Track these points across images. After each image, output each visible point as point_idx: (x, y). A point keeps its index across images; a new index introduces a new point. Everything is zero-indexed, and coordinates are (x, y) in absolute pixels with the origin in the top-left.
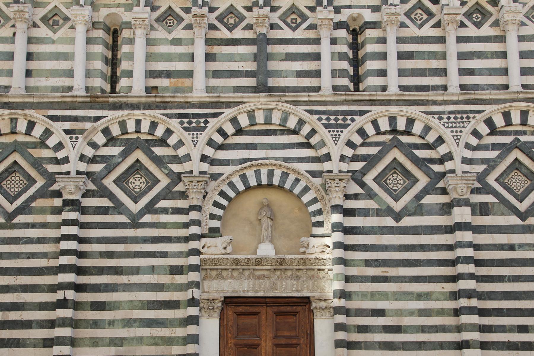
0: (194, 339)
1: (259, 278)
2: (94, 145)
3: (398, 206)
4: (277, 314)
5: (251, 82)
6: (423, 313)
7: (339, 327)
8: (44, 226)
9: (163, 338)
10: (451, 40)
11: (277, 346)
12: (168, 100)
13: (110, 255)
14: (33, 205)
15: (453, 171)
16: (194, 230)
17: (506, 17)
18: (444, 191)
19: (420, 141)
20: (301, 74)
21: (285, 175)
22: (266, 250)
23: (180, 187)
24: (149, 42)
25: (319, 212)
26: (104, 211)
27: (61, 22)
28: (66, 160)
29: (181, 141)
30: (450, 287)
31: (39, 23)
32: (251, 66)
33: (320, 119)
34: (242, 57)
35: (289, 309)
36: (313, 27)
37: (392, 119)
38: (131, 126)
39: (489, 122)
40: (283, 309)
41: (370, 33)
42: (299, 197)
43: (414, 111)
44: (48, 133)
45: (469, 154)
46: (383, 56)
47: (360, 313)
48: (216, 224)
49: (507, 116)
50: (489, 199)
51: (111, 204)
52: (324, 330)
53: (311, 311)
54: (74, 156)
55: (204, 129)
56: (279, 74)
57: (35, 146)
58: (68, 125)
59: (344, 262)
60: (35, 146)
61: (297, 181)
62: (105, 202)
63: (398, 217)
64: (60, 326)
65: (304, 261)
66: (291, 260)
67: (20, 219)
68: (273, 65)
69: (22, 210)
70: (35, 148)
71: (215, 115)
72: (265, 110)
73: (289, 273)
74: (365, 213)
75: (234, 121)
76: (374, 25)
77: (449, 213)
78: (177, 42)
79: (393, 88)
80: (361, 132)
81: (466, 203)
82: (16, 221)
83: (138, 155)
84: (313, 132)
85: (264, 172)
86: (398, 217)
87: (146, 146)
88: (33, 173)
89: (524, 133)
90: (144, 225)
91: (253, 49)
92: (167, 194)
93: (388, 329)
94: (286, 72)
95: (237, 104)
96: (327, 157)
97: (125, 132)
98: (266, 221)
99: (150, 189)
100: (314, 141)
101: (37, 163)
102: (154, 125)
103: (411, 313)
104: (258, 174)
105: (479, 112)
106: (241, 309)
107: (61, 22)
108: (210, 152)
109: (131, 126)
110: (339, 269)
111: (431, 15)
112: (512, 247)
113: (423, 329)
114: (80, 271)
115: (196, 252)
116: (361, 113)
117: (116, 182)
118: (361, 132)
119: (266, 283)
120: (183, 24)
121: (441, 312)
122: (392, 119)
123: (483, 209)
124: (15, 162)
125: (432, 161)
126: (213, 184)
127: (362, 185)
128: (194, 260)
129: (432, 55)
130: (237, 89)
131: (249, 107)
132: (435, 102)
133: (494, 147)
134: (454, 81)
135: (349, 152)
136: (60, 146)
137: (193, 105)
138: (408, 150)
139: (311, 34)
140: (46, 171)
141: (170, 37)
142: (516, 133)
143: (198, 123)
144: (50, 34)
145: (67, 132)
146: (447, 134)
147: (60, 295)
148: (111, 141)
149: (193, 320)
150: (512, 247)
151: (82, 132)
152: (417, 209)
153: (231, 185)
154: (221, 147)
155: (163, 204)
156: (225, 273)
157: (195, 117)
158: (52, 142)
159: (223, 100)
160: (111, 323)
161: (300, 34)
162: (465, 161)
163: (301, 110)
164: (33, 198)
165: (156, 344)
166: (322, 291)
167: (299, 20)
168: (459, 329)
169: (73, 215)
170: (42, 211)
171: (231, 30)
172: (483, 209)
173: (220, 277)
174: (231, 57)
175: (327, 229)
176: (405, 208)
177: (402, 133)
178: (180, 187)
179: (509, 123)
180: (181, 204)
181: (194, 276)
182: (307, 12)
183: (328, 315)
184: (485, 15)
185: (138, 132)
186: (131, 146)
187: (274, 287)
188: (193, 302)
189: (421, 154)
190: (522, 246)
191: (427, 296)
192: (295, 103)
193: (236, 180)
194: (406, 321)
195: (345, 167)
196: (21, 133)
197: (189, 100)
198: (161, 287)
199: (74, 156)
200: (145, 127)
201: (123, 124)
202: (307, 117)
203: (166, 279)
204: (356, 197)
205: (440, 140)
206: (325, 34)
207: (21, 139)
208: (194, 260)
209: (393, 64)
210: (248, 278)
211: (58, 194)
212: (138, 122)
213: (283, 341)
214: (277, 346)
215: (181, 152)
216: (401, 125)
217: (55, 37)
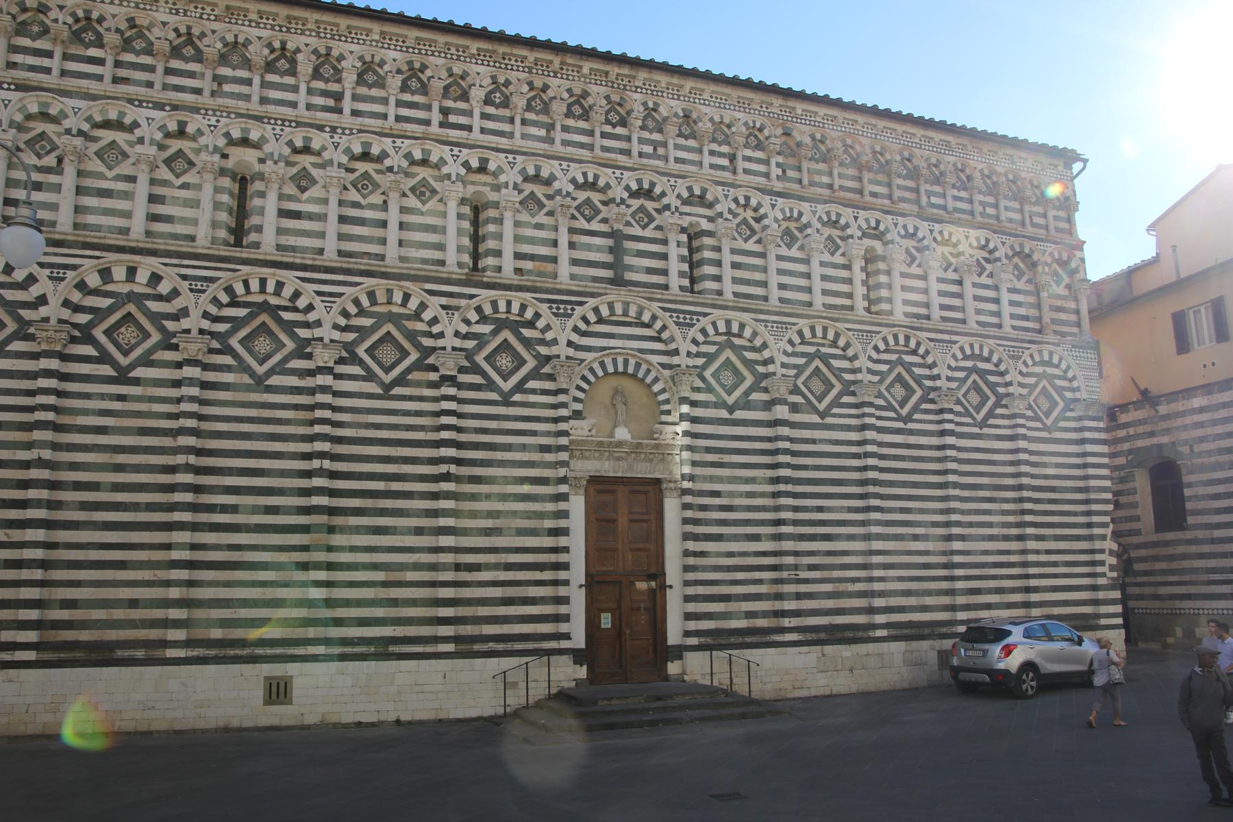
0: (564, 514)
1: (618, 459)
2: (467, 322)
3: (730, 400)
4: (632, 492)
5: (608, 274)
6: (750, 495)
7: (686, 506)
8: (421, 399)
9: (535, 512)
10: (772, 257)
11: (631, 521)
12: (539, 284)
14: (409, 377)
15: (774, 374)
16: (564, 412)
17: (813, 245)
18: (766, 390)
19: (748, 344)
20: (650, 271)
21: (638, 365)
22: (622, 434)
23: (547, 370)
24: (517, 224)
25: (667, 401)
26: (478, 387)
27: (428, 194)
28: (441, 335)
29: (548, 325)
30: (770, 473)
31: (408, 193)
32: (607, 258)
33: (671, 317)
34: (599, 249)
35: (641, 488)
36: (659, 228)
37: (728, 323)
38: (502, 307)
39: (800, 333)
40: (636, 488)
41: (707, 241)
42: (649, 386)
43: (746, 317)
44: (423, 306)
45: (786, 360)
46: (718, 263)
47: (702, 493)
48: (578, 407)
49: (813, 329)
50: (798, 399)
51: (484, 382)
52: (672, 508)
53: (661, 490)
54: (449, 332)
55: (570, 316)
56: (631, 268)
57: (409, 317)
58: (444, 301)
59: (690, 448)
60: (409, 317)
61: (649, 371)
62: (478, 379)
63: (731, 410)
64: (444, 499)
65: (657, 446)
66: (647, 445)
67: (397, 391)
68: (628, 260)
69: (400, 381)
70: (409, 320)
71: (581, 304)
72: (623, 302)
73: (643, 456)
74: (705, 405)
75: (596, 310)
76: (710, 234)
77: (770, 410)
78: (539, 226)
79: (728, 295)
80: (703, 331)
81: (784, 402)
82: (393, 392)
83: (506, 334)
84: (664, 327)
85: (620, 360)
86: (731, 410)
87: (515, 327)
88: (406, 345)
89: (823, 345)
90: (515, 404)
91: (610, 242)
92: (535, 374)
93: (723, 508)
94: (638, 267)
95: (600, 295)
96: (676, 352)
97: (496, 310)
98: (621, 408)
99: (517, 369)
100: (665, 335)
101: (412, 336)
102: (523, 307)
103: (741, 495)
104: (615, 361)
105: (795, 324)
106: (601, 487)
107: (428, 194)
108: (575, 338)
109: (502, 307)
110: (686, 455)
111: (753, 232)
112: (814, 441)
113: (749, 509)
114: (459, 445)
115: (565, 433)
116: (705, 315)
117: (487, 359)
118: (703, 331)
119: (623, 464)
120: (545, 210)
121: (763, 495)
122: (728, 323)
124: (388, 333)
125: (757, 362)
126: (577, 369)
127: (703, 379)
128: (563, 441)
129: (754, 268)
130: (595, 279)
131: (610, 298)
132: (762, 312)
133: (803, 355)
134: (775, 294)
135: (694, 349)
136: (435, 321)
137: (560, 292)
138: (737, 350)
139: (658, 235)
140: (421, 344)
141: (534, 221)
142: (818, 345)
143: (565, 309)
144: (419, 205)
145: (444, 307)
146: (771, 341)
147: (443, 468)
148: (483, 319)
149: (563, 497)
150: (814, 441)
151: (457, 308)
152: (748, 406)
153: (592, 370)
155: (532, 384)
156: (587, 454)
157: (563, 302)
158: (427, 316)
159: (588, 290)
160: (488, 497)
161: (648, 233)
162: (783, 365)
163: (656, 305)
164: (409, 370)
165: (529, 518)
166: (671, 473)
167: (646, 220)
168: (777, 509)
169: (452, 391)
170: (418, 384)
171: (589, 221)
172: (795, 408)
173: (583, 457)
174: (588, 248)
175: (674, 417)
176: (736, 402)
177: (735, 335)
178: (547, 370)
179: (814, 336)
180: (548, 385)
181: (564, 456)
182: (654, 214)
183: (675, 494)
184: (793, 239)
185: (508, 312)
186: (501, 325)
187: (630, 468)
188: (563, 480)
189: (750, 355)
190: (822, 441)
191: (752, 480)
193: (596, 366)
194: (737, 502)
195: (691, 362)
196: (396, 304)
197: (558, 286)
199: (449, 332)
200: (515, 308)
201: (494, 304)
202: (660, 313)
203: (536, 457)
204: (698, 390)
205: (765, 346)
206: (673, 237)
207: (395, 309)
208: (563, 441)
209: (728, 273)
210: (608, 459)
211: (434, 369)
212: (509, 303)
213: (636, 517)
214: (631, 521)
215: (549, 336)
216: (735, 329)
217: (424, 209)
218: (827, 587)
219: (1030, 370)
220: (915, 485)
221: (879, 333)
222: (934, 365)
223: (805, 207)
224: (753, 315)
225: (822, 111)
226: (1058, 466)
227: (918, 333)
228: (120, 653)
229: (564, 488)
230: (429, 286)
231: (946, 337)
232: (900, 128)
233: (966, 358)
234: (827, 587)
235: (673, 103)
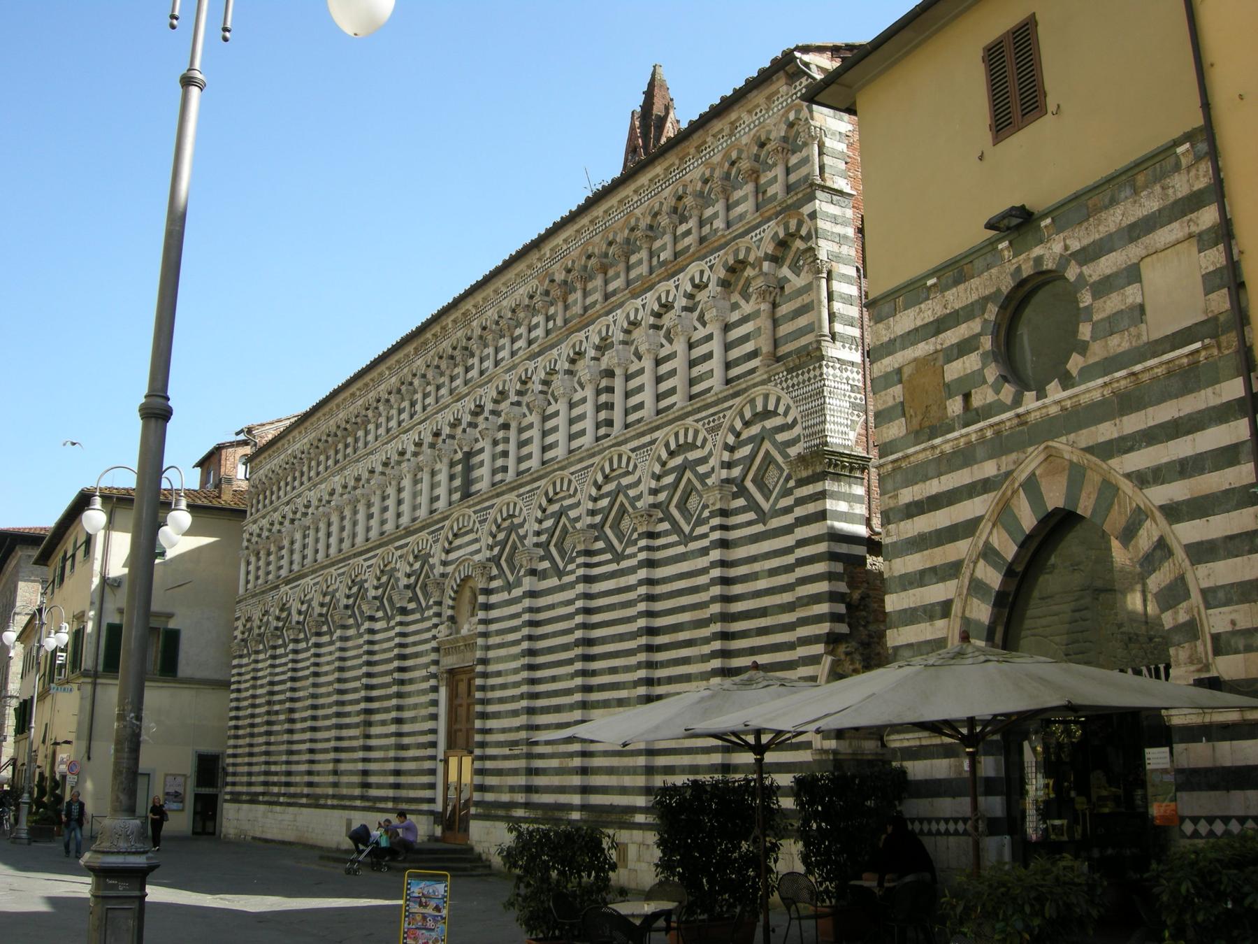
0: (435, 703)
13: (415, 644)
48: (450, 612)
89: (564, 498)
112: (552, 607)
115: (434, 637)
118: (496, 520)
123: (543, 575)
145: (400, 557)
154: (448, 552)
192: (469, 507)
198: (427, 666)
208: (434, 644)
218: (554, 763)
219: (744, 436)
220: (621, 638)
221: (592, 465)
222: (639, 481)
223: (555, 351)
224: (515, 493)
225: (559, 240)
226: (773, 572)
227: (623, 448)
228: (322, 802)
229: (433, 682)
230: (397, 544)
231: (647, 439)
232: (613, 201)
233: (672, 454)
234: (554, 763)
235: (489, 313)
